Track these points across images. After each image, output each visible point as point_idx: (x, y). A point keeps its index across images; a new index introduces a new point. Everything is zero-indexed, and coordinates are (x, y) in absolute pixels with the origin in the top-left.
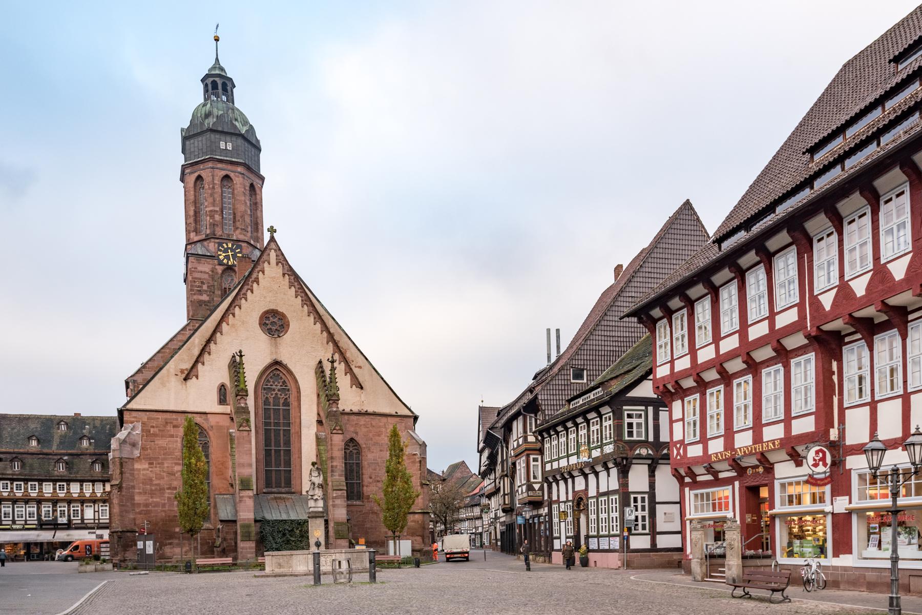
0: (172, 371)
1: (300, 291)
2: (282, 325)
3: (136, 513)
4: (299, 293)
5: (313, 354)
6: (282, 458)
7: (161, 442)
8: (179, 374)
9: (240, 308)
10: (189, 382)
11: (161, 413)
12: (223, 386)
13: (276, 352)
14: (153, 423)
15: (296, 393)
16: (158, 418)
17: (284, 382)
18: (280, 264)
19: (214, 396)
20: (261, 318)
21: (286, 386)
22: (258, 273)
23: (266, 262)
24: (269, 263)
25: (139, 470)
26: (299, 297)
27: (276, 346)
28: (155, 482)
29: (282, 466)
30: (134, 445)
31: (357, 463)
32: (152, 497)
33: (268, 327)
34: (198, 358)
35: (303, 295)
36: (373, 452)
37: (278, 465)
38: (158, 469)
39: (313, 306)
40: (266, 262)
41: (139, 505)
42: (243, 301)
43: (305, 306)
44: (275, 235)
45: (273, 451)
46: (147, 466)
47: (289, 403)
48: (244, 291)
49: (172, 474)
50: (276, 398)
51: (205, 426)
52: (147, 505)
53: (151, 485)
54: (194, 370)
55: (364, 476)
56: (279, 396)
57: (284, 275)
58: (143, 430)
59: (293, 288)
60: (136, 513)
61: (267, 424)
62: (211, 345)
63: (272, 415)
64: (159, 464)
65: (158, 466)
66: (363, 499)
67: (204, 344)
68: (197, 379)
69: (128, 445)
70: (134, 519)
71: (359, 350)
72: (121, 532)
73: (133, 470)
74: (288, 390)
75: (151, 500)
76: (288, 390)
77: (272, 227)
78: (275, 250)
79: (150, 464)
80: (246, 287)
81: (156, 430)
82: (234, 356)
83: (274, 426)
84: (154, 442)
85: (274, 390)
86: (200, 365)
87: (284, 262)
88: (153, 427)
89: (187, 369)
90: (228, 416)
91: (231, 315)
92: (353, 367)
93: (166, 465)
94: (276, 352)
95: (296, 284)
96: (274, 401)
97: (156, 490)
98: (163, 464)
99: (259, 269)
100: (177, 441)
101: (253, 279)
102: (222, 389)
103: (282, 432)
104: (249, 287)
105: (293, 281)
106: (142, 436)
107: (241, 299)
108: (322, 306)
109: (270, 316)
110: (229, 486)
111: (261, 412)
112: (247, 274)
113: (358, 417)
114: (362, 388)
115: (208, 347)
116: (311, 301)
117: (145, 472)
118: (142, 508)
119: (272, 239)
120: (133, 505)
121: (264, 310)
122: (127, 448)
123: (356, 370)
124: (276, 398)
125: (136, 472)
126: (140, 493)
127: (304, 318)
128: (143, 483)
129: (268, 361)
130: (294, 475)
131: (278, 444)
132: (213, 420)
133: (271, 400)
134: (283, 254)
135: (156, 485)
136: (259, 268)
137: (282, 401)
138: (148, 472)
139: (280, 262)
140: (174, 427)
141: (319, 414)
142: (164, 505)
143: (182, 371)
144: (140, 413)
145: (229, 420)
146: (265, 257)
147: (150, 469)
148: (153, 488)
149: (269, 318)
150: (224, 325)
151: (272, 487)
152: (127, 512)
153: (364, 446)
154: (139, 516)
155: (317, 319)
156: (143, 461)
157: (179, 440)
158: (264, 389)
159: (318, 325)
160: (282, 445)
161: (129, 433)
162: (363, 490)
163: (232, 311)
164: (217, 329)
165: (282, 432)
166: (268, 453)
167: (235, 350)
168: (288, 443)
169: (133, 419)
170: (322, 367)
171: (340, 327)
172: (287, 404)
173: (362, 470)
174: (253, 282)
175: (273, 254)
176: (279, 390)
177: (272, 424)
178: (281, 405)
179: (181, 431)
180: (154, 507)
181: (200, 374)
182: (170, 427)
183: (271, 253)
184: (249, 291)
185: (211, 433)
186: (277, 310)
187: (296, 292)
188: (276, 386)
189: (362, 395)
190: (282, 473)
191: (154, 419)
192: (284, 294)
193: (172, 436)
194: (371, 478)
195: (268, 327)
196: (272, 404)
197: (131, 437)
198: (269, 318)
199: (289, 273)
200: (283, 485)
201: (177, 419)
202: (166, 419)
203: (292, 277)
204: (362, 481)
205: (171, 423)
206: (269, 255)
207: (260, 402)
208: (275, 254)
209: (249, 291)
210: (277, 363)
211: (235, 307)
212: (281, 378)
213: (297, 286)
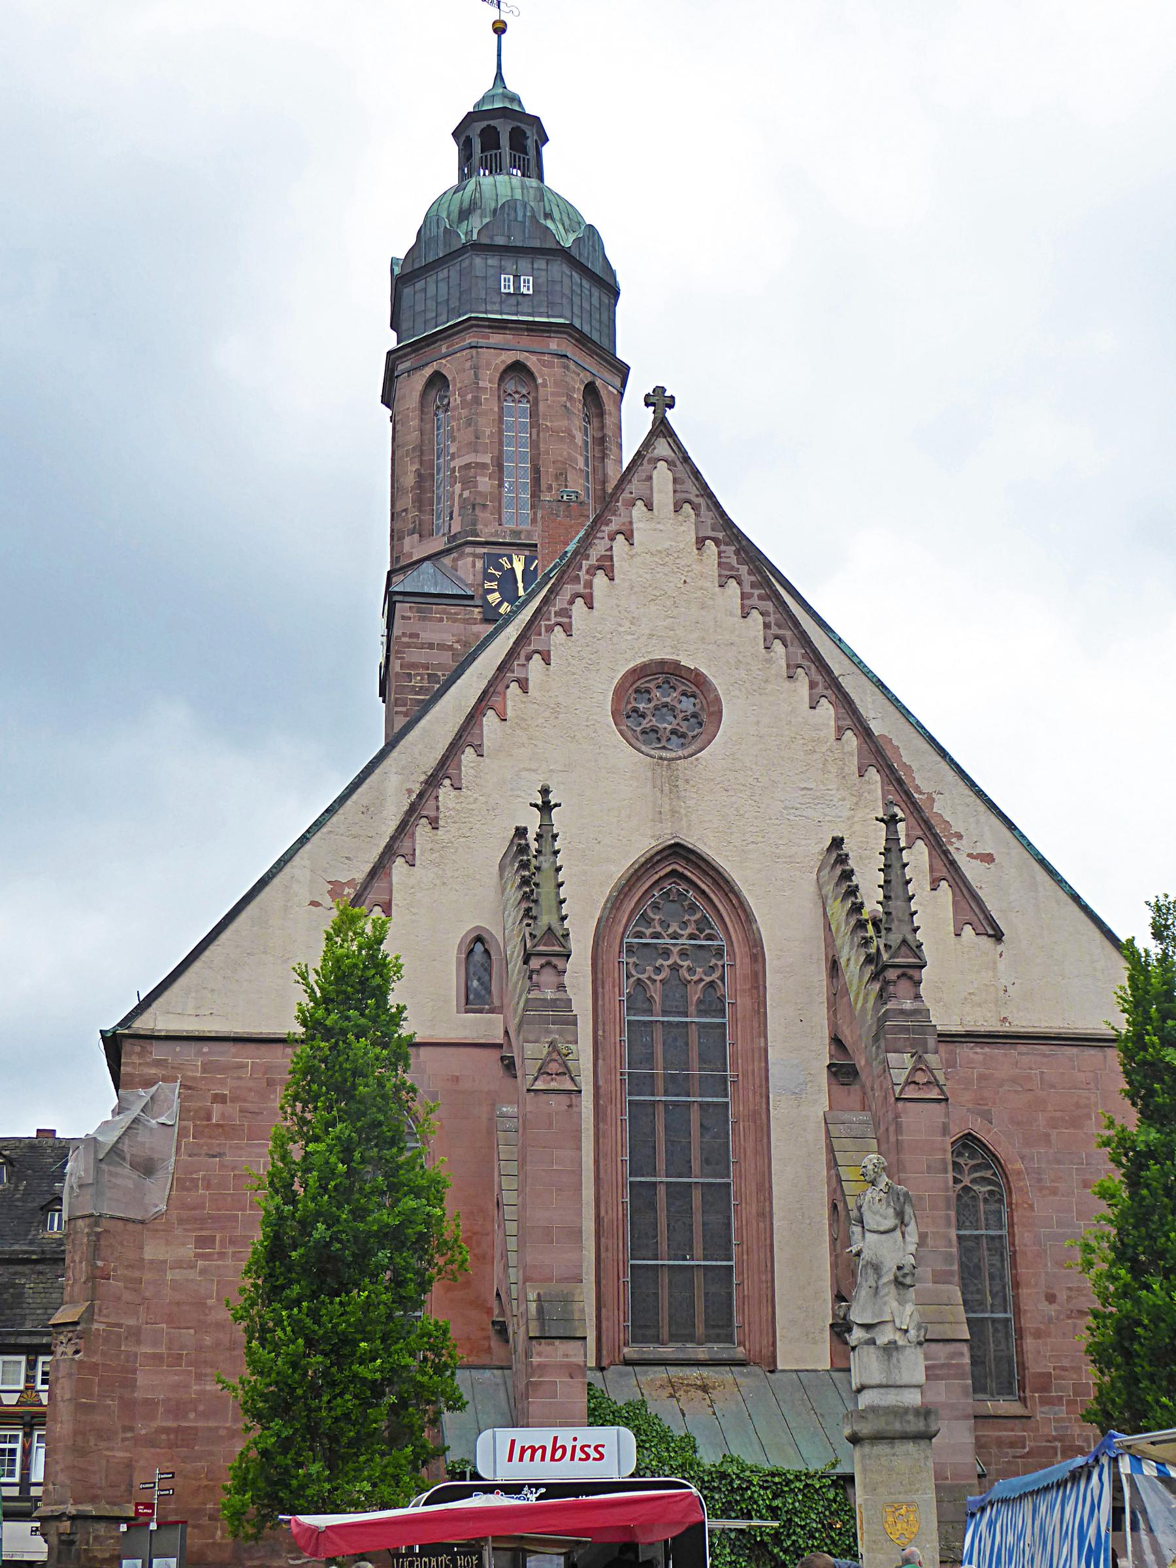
0: (303, 894)
1: (756, 592)
2: (694, 715)
3: (138, 1441)
4: (755, 601)
5: (809, 812)
6: (698, 1218)
8: (327, 901)
9: (547, 661)
11: (252, 1046)
12: (479, 939)
13: (673, 812)
14: (222, 1082)
15: (747, 960)
16: (243, 1066)
17: (703, 923)
18: (687, 506)
20: (619, 693)
21: (710, 937)
22: (612, 539)
23: (639, 503)
24: (649, 507)
25: (160, 1266)
26: (755, 613)
27: (672, 787)
29: (698, 1250)
30: (147, 1168)
31: (992, 1238)
33: (645, 724)
34: (393, 838)
35: (769, 606)
36: (1054, 1192)
37: (683, 1248)
38: (229, 1262)
39: (805, 639)
40: (639, 503)
41: (150, 1404)
43: (778, 646)
44: (669, 414)
45: (662, 1191)
46: (189, 1251)
47: (721, 999)
48: (560, 602)
50: (677, 982)
52: (178, 1409)
54: (377, 884)
55: (1023, 1291)
56: (684, 973)
57: (700, 542)
58: (184, 1112)
59: (733, 583)
60: (138, 1441)
61: (639, 1083)
62: (441, 791)
63: (659, 1050)
64: (232, 1242)
65: (230, 1250)
66: (1022, 1388)
69: (126, 1170)
70: (129, 1465)
71: (980, 794)
72: (73, 1518)
73: (140, 1264)
74: (719, 953)
76: (719, 953)
77: (659, 390)
78: (671, 464)
79: (202, 1242)
80: (568, 590)
81: (232, 1109)
82: (521, 832)
83: (666, 1094)
84: (220, 1155)
85: (666, 953)
86: (399, 866)
87: (700, 500)
88: (220, 1099)
89: (350, 883)
90: (495, 1055)
91: (514, 685)
92: (962, 860)
94: (673, 812)
95: (744, 569)
96: (665, 997)
97: (217, 1344)
99: (613, 527)
101: (593, 561)
103: (695, 1116)
104: (580, 588)
105: (733, 561)
106: (183, 1133)
107: (550, 629)
108: (838, 642)
109: (651, 685)
110: (491, 1331)
111: (618, 1037)
112: (571, 548)
113: (987, 1050)
114: (998, 936)
115: (432, 802)
116: (796, 624)
118: (160, 1422)
119: (662, 429)
120: (128, 1406)
121: (631, 665)
122: (126, 1176)
123: (972, 870)
124: (677, 982)
125: (148, 1276)
126: (158, 1358)
127: (769, 687)
128: (170, 1320)
129: (643, 845)
130: (744, 1285)
131: (679, 1162)
133: (656, 992)
134: (696, 474)
137: (696, 994)
138: (192, 1274)
139: (689, 502)
141: (837, 1041)
143: (336, 889)
144: (178, 1047)
145: (498, 1069)
148: (208, 1340)
149: (648, 691)
150: (490, 720)
151: (657, 1340)
152: (104, 1434)
153: (1019, 1165)
154: (147, 1452)
155: (820, 689)
156: (178, 1231)
158: (630, 950)
159: (827, 710)
160: (696, 1165)
161: (136, 1121)
162: (1021, 1352)
163: (518, 673)
165: (695, 1116)
166: (642, 1196)
168: (717, 1159)
169: (153, 1071)
170: (843, 859)
171: (905, 713)
172: (713, 1003)
173: (1014, 1265)
174: (592, 571)
175: (662, 476)
176: (683, 954)
177: (660, 1084)
178: (692, 1009)
183: (655, 474)
184: (579, 601)
186: (677, 664)
187: (744, 596)
188: (675, 936)
189: (1002, 965)
190: (699, 1278)
191: (224, 1069)
192: (703, 607)
194: (1051, 1298)
195: (645, 724)
196: (657, 1007)
197: (142, 1137)
198: (648, 691)
199: (720, 535)
200: (700, 1330)
202: (268, 1068)
203: (730, 549)
204: (1018, 1312)
206: (650, 478)
207: (615, 998)
209: (579, 601)
210: (678, 851)
211: (529, 658)
212: (693, 908)
213: (747, 579)
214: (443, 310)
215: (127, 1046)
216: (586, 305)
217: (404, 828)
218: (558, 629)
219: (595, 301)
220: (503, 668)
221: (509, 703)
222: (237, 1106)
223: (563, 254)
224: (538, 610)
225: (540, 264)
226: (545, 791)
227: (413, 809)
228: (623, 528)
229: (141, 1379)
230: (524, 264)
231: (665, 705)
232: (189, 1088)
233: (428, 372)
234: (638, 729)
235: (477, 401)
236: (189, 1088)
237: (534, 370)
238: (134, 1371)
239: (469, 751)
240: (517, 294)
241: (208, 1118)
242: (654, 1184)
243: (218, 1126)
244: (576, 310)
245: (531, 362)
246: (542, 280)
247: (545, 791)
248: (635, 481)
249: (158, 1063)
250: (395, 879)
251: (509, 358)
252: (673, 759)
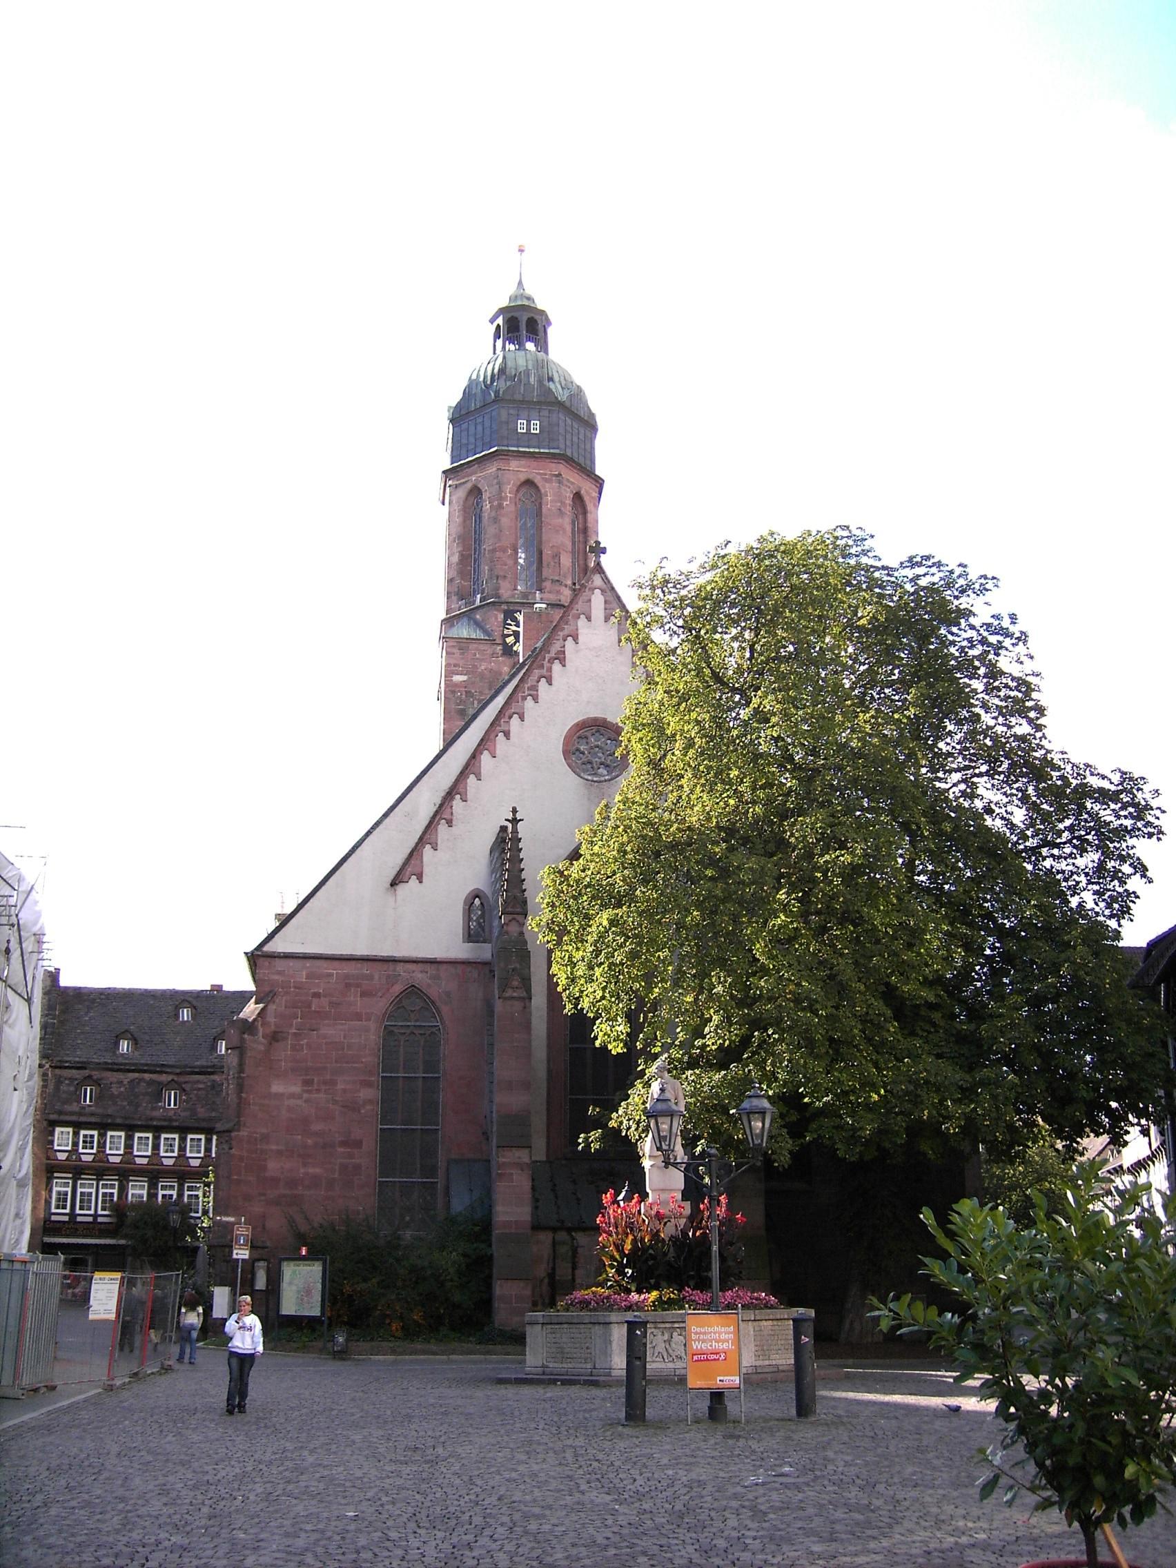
7: (332, 1031)
9: (522, 718)
10: (402, 889)
16: (331, 975)
24: (589, 619)
25: (279, 1096)
28: (317, 1127)
32: (305, 1165)
41: (275, 1181)
42: (529, 702)
46: (296, 1089)
49: (352, 1107)
51: (433, 992)
52: (293, 1183)
62: (454, 803)
64: (325, 1083)
65: (323, 1087)
67: (439, 801)
68: (421, 882)
75: (302, 1171)
78: (603, 591)
79: (307, 1083)
80: (537, 672)
81: (324, 1001)
88: (317, 995)
91: (501, 735)
93: (340, 1086)
98: (334, 1083)
99: (566, 632)
101: (552, 654)
104: (544, 672)
107: (524, 698)
109: (588, 734)
112: (539, 644)
117: (292, 1102)
126: (280, 1153)
136: (567, 629)
138: (299, 1102)
140: (363, 994)
144: (291, 963)
146: (580, 606)
147: (305, 1096)
150: (485, 757)
167: (502, 817)
174: (551, 661)
175: (598, 600)
179: (380, 1005)
181: (427, 870)
182: (355, 996)
183: (593, 598)
185: (445, 1010)
186: (605, 720)
191: (319, 977)
193: (358, 1017)
198: (586, 737)
201: (371, 977)
202: (347, 976)
205: (358, 986)
206: (590, 600)
208: (602, 599)
211: (510, 717)
214: (479, 443)
215: (260, 961)
216: (575, 439)
218: (529, 698)
219: (581, 437)
220: (494, 723)
221: (498, 746)
222: (327, 999)
223: (561, 405)
224: (517, 686)
226: (514, 811)
227: (436, 813)
228: (572, 633)
230: (534, 414)
231: (597, 746)
232: (299, 988)
233: (469, 485)
234: (579, 762)
236: (299, 988)
237: (539, 485)
238: (265, 1160)
239: (472, 776)
241: (310, 1007)
242: (585, 1049)
243: (315, 1012)
244: (568, 443)
245: (538, 480)
246: (545, 424)
247: (514, 811)
248: (580, 603)
249: (279, 973)
250: (425, 859)
251: (523, 477)
252: (600, 782)
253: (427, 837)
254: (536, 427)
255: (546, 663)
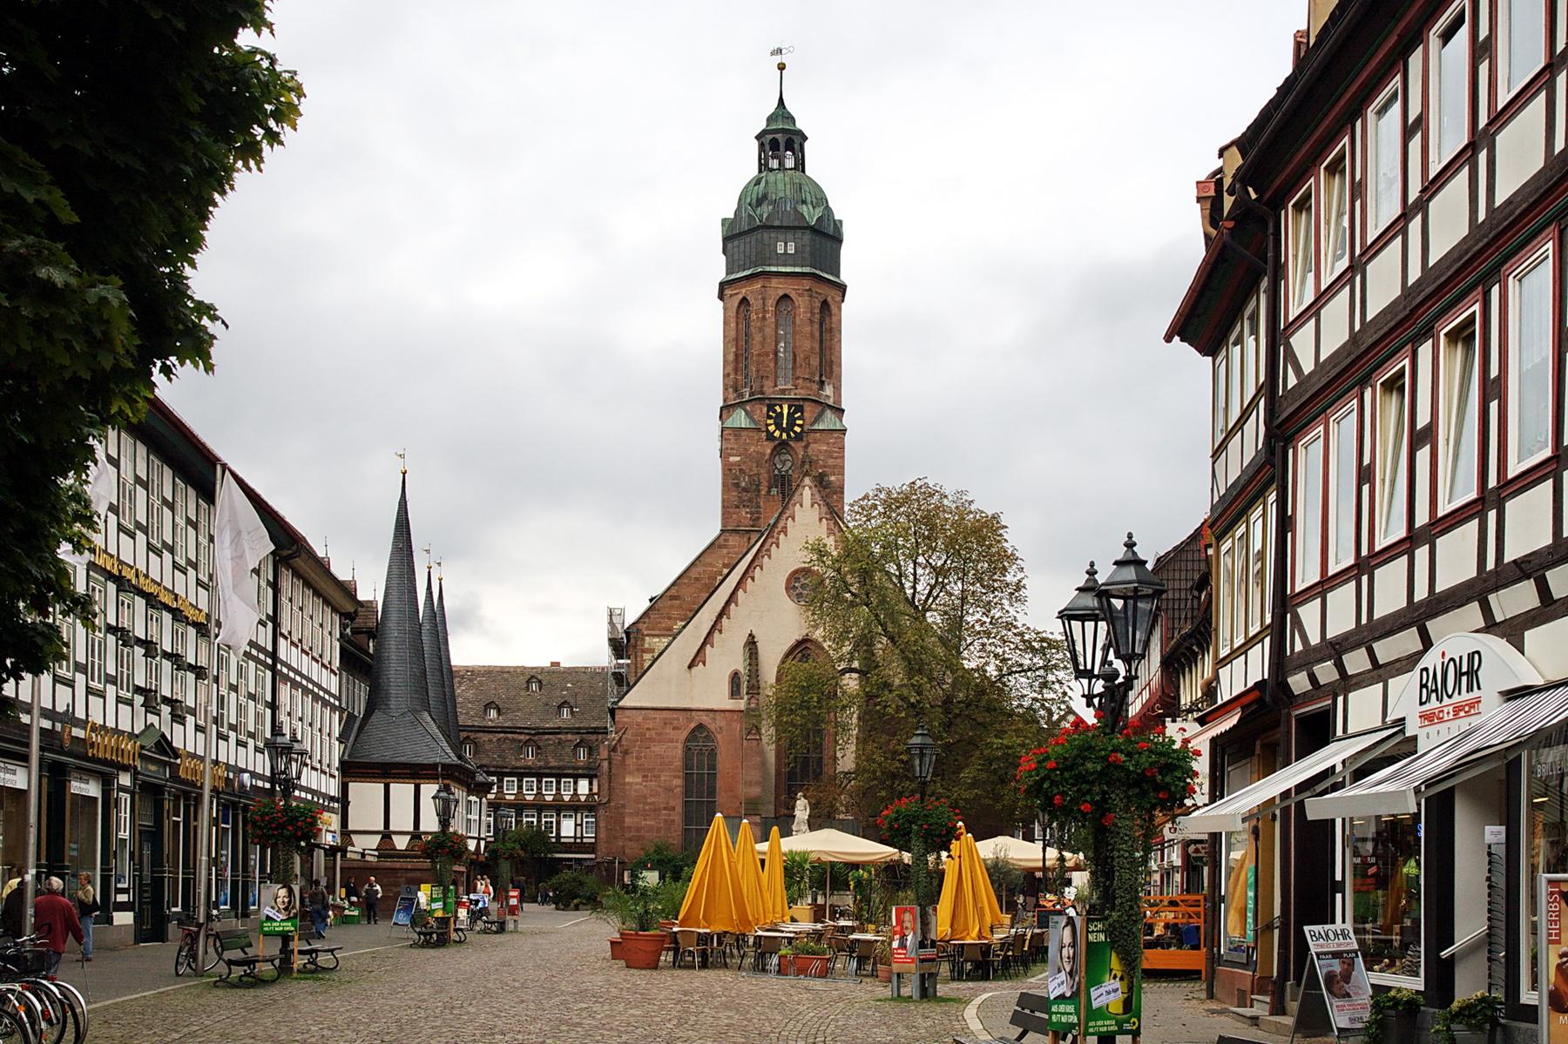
7: (657, 749)
10: (694, 669)
16: (655, 718)
19: (725, 688)
24: (801, 506)
25: (630, 784)
28: (649, 801)
32: (645, 820)
34: (705, 639)
46: (640, 780)
48: (767, 547)
49: (669, 790)
51: (712, 727)
52: (638, 829)
53: (645, 803)
70: (623, 847)
73: (625, 784)
79: (644, 776)
80: (770, 540)
81: (653, 732)
88: (649, 729)
97: (650, 809)
98: (660, 776)
100: (677, 748)
101: (779, 529)
102: (735, 677)
107: (763, 557)
112: (772, 522)
117: (637, 787)
118: (632, 834)
132: (720, 722)
135: (650, 804)
140: (673, 729)
142: (659, 830)
152: (615, 838)
157: (680, 746)
164: (732, 598)
174: (779, 533)
180: (649, 831)
199: (828, 516)
201: (678, 719)
202: (665, 719)
205: (671, 724)
217: (710, 634)
224: (759, 550)
225: (799, 234)
227: (713, 626)
229: (626, 819)
230: (790, 236)
235: (764, 318)
240: (786, 253)
253: (708, 639)
254: (791, 250)
255: (775, 535)
